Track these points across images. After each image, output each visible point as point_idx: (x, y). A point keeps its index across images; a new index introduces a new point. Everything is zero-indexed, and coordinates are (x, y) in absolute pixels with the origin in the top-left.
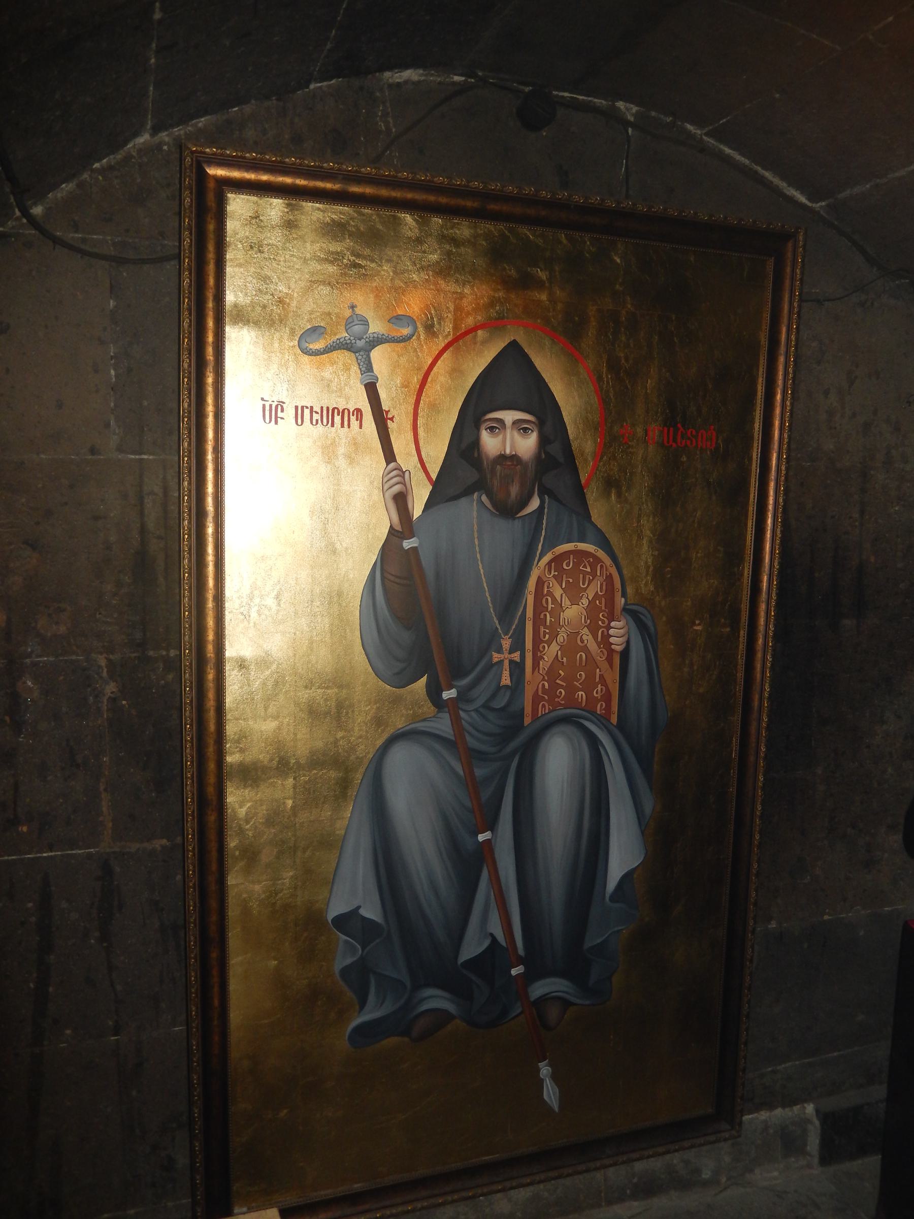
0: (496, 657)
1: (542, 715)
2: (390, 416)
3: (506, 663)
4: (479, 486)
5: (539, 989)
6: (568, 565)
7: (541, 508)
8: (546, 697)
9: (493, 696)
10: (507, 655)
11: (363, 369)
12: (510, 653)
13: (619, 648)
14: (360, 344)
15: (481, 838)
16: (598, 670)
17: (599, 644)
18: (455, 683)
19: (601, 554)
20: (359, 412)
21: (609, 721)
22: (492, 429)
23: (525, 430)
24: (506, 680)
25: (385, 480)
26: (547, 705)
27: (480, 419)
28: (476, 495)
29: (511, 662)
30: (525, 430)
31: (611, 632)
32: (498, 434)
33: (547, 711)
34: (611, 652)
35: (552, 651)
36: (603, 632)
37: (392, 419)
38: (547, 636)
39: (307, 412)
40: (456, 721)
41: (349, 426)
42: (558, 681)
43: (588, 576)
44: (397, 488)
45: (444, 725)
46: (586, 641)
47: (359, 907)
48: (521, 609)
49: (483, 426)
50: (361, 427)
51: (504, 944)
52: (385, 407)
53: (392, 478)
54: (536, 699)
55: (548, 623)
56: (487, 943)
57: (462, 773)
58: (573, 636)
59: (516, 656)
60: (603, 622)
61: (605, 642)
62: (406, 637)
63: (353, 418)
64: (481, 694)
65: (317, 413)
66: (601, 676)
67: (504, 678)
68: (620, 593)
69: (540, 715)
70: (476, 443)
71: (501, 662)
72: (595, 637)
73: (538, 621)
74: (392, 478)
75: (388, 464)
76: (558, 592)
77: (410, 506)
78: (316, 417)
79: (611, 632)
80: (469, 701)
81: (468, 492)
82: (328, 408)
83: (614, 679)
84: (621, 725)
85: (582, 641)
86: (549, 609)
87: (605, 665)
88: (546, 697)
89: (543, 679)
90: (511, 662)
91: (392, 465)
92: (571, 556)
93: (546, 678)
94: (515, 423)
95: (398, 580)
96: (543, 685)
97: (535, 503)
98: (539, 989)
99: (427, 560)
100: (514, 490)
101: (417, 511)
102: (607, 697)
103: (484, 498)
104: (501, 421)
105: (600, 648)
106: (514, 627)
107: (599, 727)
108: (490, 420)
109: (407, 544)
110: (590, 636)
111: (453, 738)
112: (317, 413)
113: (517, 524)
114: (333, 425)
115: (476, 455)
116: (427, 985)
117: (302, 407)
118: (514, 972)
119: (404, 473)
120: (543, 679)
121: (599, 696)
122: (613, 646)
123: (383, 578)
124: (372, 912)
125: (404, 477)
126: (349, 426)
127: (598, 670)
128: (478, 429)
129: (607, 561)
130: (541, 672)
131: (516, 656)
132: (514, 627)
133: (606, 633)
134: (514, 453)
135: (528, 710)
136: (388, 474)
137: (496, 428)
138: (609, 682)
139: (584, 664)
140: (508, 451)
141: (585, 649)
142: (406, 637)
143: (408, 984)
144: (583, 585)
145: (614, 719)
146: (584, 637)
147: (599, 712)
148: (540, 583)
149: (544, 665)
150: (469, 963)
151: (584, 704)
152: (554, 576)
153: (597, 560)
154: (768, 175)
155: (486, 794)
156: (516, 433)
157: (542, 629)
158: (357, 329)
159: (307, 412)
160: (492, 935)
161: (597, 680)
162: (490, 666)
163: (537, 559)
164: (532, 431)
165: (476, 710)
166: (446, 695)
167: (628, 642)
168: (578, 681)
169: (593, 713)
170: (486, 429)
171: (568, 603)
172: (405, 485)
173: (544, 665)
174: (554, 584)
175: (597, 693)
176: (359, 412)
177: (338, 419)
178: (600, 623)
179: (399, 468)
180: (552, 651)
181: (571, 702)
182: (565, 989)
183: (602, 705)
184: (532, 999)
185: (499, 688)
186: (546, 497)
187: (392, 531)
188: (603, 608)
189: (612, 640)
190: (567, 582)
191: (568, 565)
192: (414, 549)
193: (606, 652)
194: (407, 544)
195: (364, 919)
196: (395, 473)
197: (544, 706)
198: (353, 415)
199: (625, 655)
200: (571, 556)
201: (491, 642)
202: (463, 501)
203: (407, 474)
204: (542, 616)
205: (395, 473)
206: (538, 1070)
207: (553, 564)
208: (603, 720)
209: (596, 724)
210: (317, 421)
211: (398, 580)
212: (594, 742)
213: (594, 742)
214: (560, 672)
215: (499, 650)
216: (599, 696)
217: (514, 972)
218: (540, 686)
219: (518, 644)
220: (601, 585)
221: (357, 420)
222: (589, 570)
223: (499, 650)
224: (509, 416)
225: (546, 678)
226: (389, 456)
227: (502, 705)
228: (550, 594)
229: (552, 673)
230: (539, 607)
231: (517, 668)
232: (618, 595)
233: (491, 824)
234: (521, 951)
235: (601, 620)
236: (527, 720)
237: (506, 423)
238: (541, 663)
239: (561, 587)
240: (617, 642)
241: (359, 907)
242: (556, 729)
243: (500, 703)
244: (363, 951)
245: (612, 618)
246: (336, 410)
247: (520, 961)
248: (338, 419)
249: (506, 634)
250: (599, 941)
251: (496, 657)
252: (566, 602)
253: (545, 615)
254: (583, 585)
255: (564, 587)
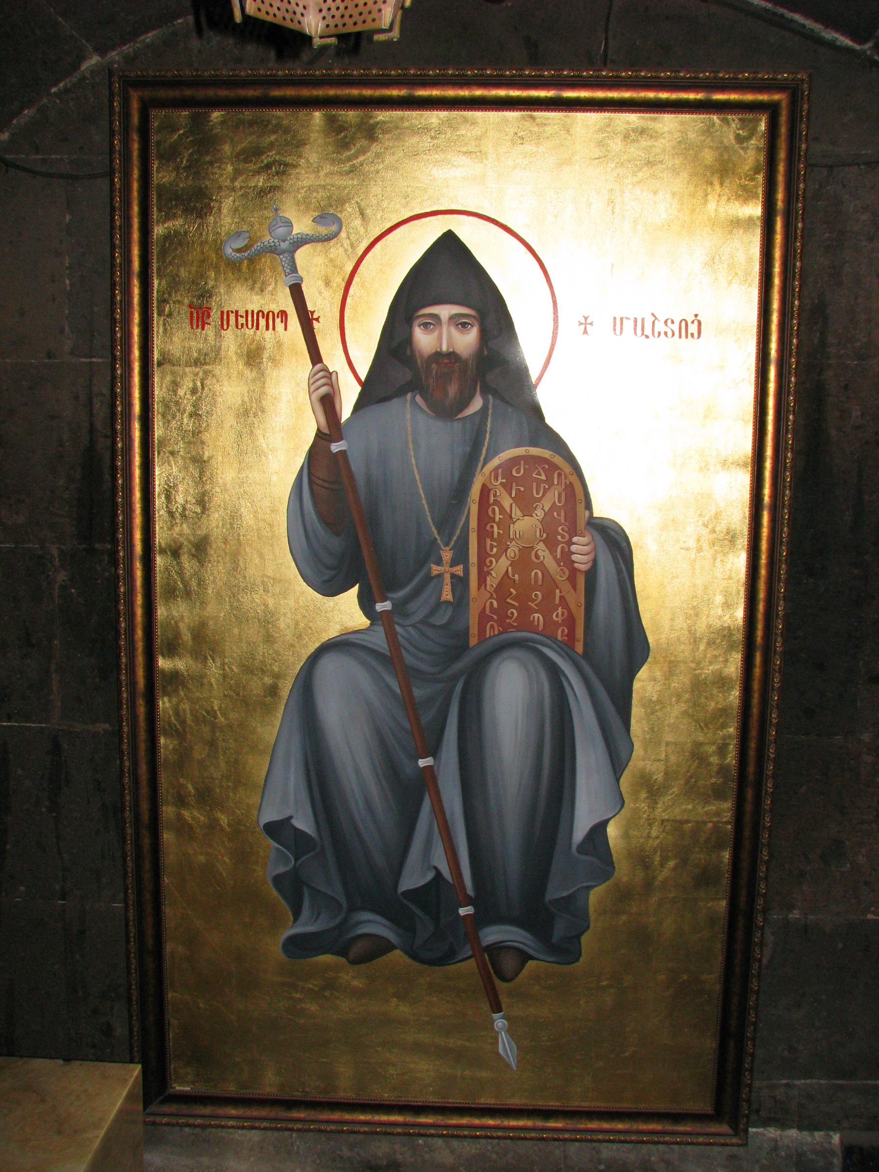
0: (435, 569)
1: (490, 637)
2: (315, 317)
3: (447, 577)
4: (415, 385)
5: (492, 935)
6: (518, 471)
7: (484, 409)
8: (495, 617)
9: (433, 612)
10: (447, 568)
11: (288, 271)
12: (451, 566)
13: (583, 567)
14: (284, 246)
15: (422, 763)
16: (557, 591)
17: (558, 562)
18: (390, 595)
19: (558, 460)
20: (283, 314)
21: (573, 648)
22: (426, 325)
23: (464, 325)
24: (447, 595)
25: (312, 381)
26: (496, 626)
27: (413, 315)
28: (409, 396)
29: (453, 576)
30: (464, 325)
31: (574, 548)
32: (432, 331)
33: (496, 632)
34: (574, 571)
35: (501, 566)
36: (563, 548)
37: (317, 320)
38: (495, 550)
39: (232, 318)
40: (391, 636)
41: (274, 329)
42: (509, 600)
43: (542, 485)
44: (324, 390)
45: (379, 640)
46: (542, 558)
47: (291, 817)
48: (464, 519)
49: (416, 323)
50: (286, 329)
51: (451, 881)
52: (310, 308)
53: (319, 379)
54: (483, 618)
55: (496, 536)
56: (430, 875)
57: (398, 691)
58: (526, 551)
59: (459, 570)
60: (563, 537)
61: (566, 558)
62: (336, 544)
63: (278, 321)
64: (419, 608)
65: (242, 317)
66: (562, 598)
67: (444, 593)
68: (583, 505)
69: (488, 635)
70: (409, 340)
71: (440, 576)
72: (552, 552)
73: (483, 534)
74: (319, 379)
75: (314, 364)
76: (507, 502)
77: (338, 408)
78: (242, 321)
79: (574, 548)
80: (407, 615)
81: (400, 392)
82: (253, 312)
83: (577, 599)
84: (586, 655)
85: (537, 557)
86: (497, 519)
87: (567, 586)
88: (495, 617)
89: (491, 597)
90: (453, 576)
91: (318, 366)
92: (522, 462)
93: (495, 596)
94: (452, 318)
95: (326, 485)
96: (491, 603)
97: (477, 404)
98: (492, 935)
99: (357, 466)
100: (453, 390)
101: (346, 412)
102: (570, 622)
103: (418, 399)
104: (436, 317)
105: (559, 566)
106: (455, 538)
107: (560, 655)
108: (424, 315)
109: (335, 447)
110: (547, 552)
111: (388, 654)
112: (242, 317)
113: (457, 426)
114: (258, 328)
115: (409, 353)
116: (364, 908)
117: (228, 312)
118: (463, 911)
119: (331, 374)
120: (491, 597)
121: (560, 619)
122: (576, 565)
123: (311, 482)
124: (304, 823)
125: (330, 378)
126: (274, 329)
127: (557, 591)
128: (411, 327)
129: (567, 468)
130: (488, 588)
131: (459, 570)
132: (455, 538)
133: (566, 549)
134: (451, 350)
135: (474, 630)
136: (316, 374)
137: (431, 324)
138: (573, 606)
139: (540, 583)
140: (444, 348)
141: (542, 566)
142: (336, 544)
143: (345, 904)
144: (538, 494)
145: (579, 648)
146: (540, 553)
147: (559, 638)
148: (485, 491)
149: (492, 581)
150: (408, 894)
151: (541, 628)
152: (502, 484)
153: (554, 467)
154: (797, 17)
155: (427, 717)
156: (453, 330)
157: (488, 542)
158: (281, 231)
159: (232, 318)
160: (436, 868)
161: (557, 601)
162: (428, 579)
163: (480, 465)
164: (472, 326)
165: (413, 626)
166: (380, 607)
167: (595, 561)
168: (533, 601)
169: (553, 638)
170: (419, 326)
171: (519, 513)
172: (331, 385)
173: (492, 581)
174: (501, 492)
175: (557, 616)
176: (283, 314)
177: (263, 322)
178: (559, 538)
179: (325, 369)
180: (501, 566)
181: (525, 624)
182: (524, 941)
183: (563, 631)
184: (484, 944)
185: (439, 604)
186: (490, 397)
187: (319, 434)
188: (563, 521)
189: (574, 557)
190: (518, 491)
191: (518, 471)
192: (343, 453)
193: (567, 573)
194: (335, 447)
195: (296, 829)
196: (321, 374)
197: (492, 627)
198: (278, 317)
199: (591, 575)
200: (522, 462)
201: (429, 553)
202: (395, 403)
203: (334, 376)
204: (488, 528)
205: (321, 374)
206: (493, 1022)
207: (500, 471)
208: (567, 647)
209: (556, 652)
210: (242, 325)
211: (326, 485)
212: (554, 673)
213: (554, 673)
214: (512, 590)
215: (439, 562)
216: (560, 619)
217: (463, 911)
218: (488, 604)
219: (461, 557)
220: (560, 495)
221: (282, 322)
222: (543, 477)
223: (439, 562)
224: (445, 311)
225: (495, 596)
226: (315, 356)
227: (444, 621)
228: (497, 503)
229: (501, 590)
230: (484, 518)
231: (460, 583)
232: (581, 507)
233: (434, 751)
234: (470, 891)
235: (559, 534)
236: (473, 641)
237: (442, 317)
238: (488, 579)
239: (510, 495)
240: (581, 559)
241: (291, 817)
242: (506, 654)
243: (441, 618)
244: (296, 860)
245: (573, 532)
246: (261, 314)
247: (469, 902)
248: (263, 322)
249: (447, 545)
250: (565, 894)
251: (435, 569)
252: (516, 513)
253: (492, 527)
254: (538, 494)
255: (513, 495)
